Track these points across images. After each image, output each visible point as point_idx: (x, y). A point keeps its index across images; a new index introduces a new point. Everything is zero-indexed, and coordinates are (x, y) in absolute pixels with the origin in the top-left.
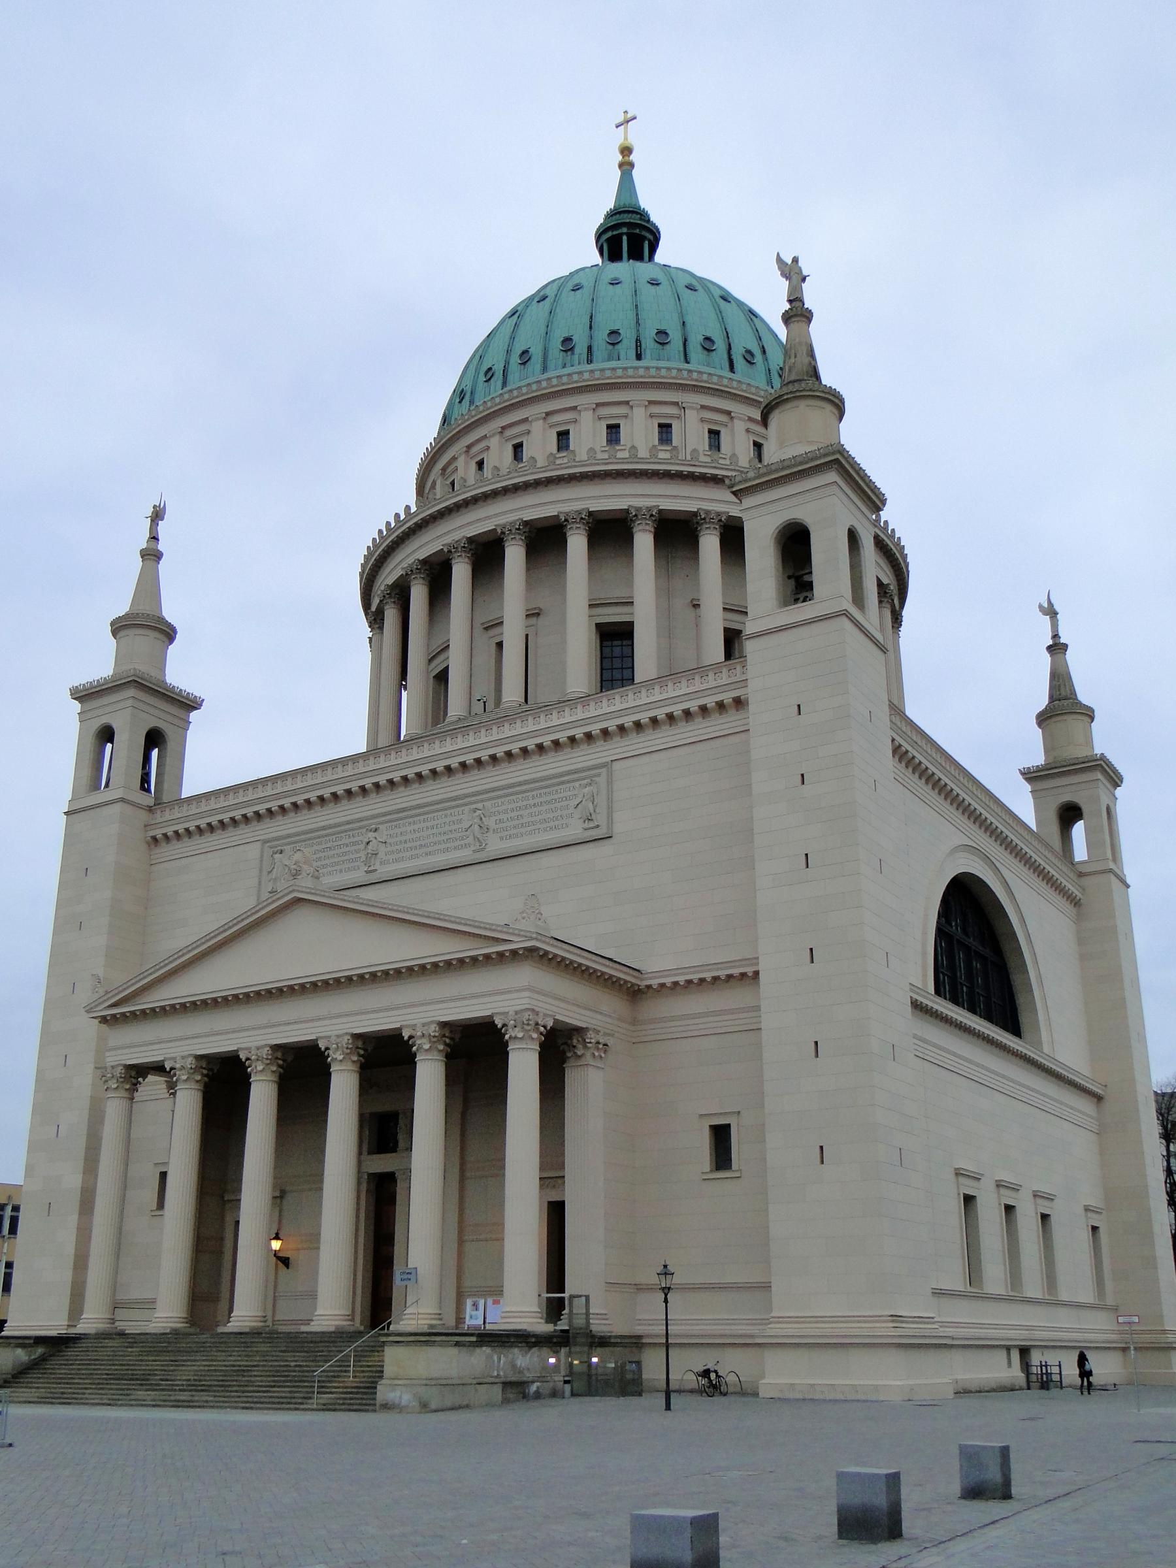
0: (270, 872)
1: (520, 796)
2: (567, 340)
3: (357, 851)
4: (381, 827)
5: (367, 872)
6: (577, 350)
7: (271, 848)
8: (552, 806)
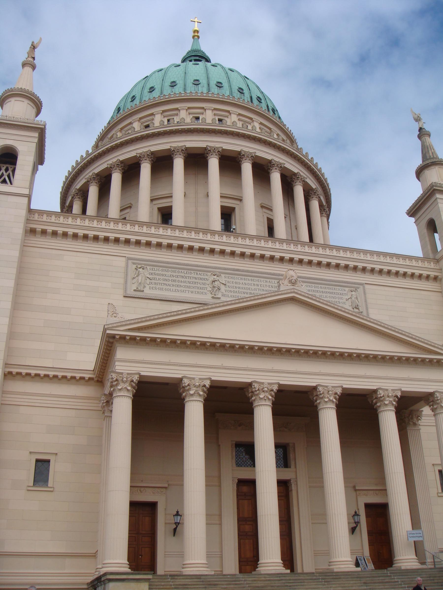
0: (134, 278)
1: (313, 285)
3: (204, 284)
4: (223, 275)
5: (213, 297)
6: (245, 94)
7: (134, 263)
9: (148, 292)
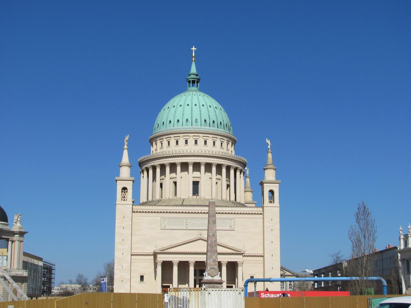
2: (205, 121)
8: (224, 223)
9: (167, 227)
